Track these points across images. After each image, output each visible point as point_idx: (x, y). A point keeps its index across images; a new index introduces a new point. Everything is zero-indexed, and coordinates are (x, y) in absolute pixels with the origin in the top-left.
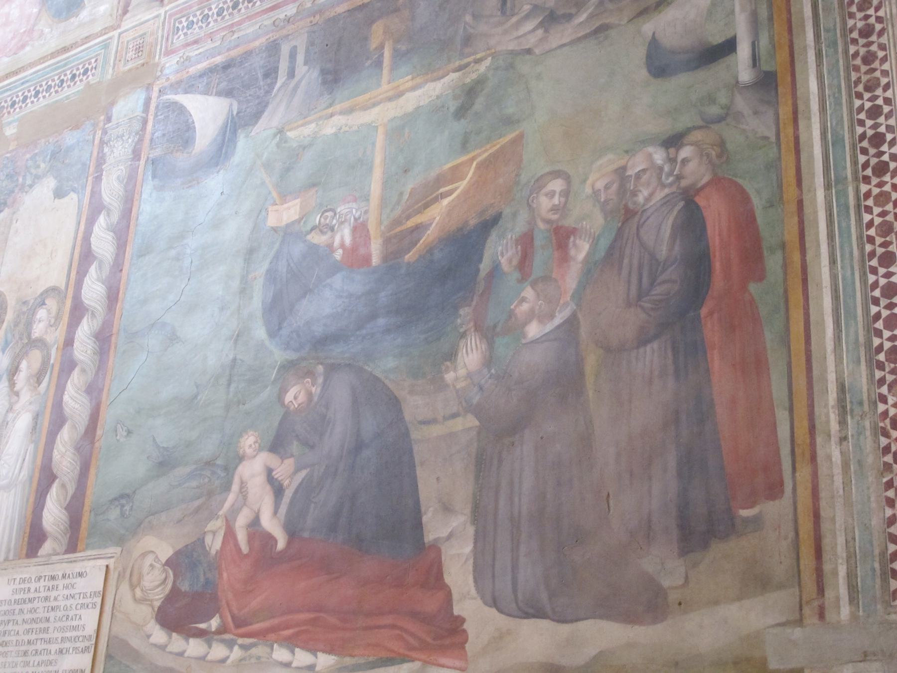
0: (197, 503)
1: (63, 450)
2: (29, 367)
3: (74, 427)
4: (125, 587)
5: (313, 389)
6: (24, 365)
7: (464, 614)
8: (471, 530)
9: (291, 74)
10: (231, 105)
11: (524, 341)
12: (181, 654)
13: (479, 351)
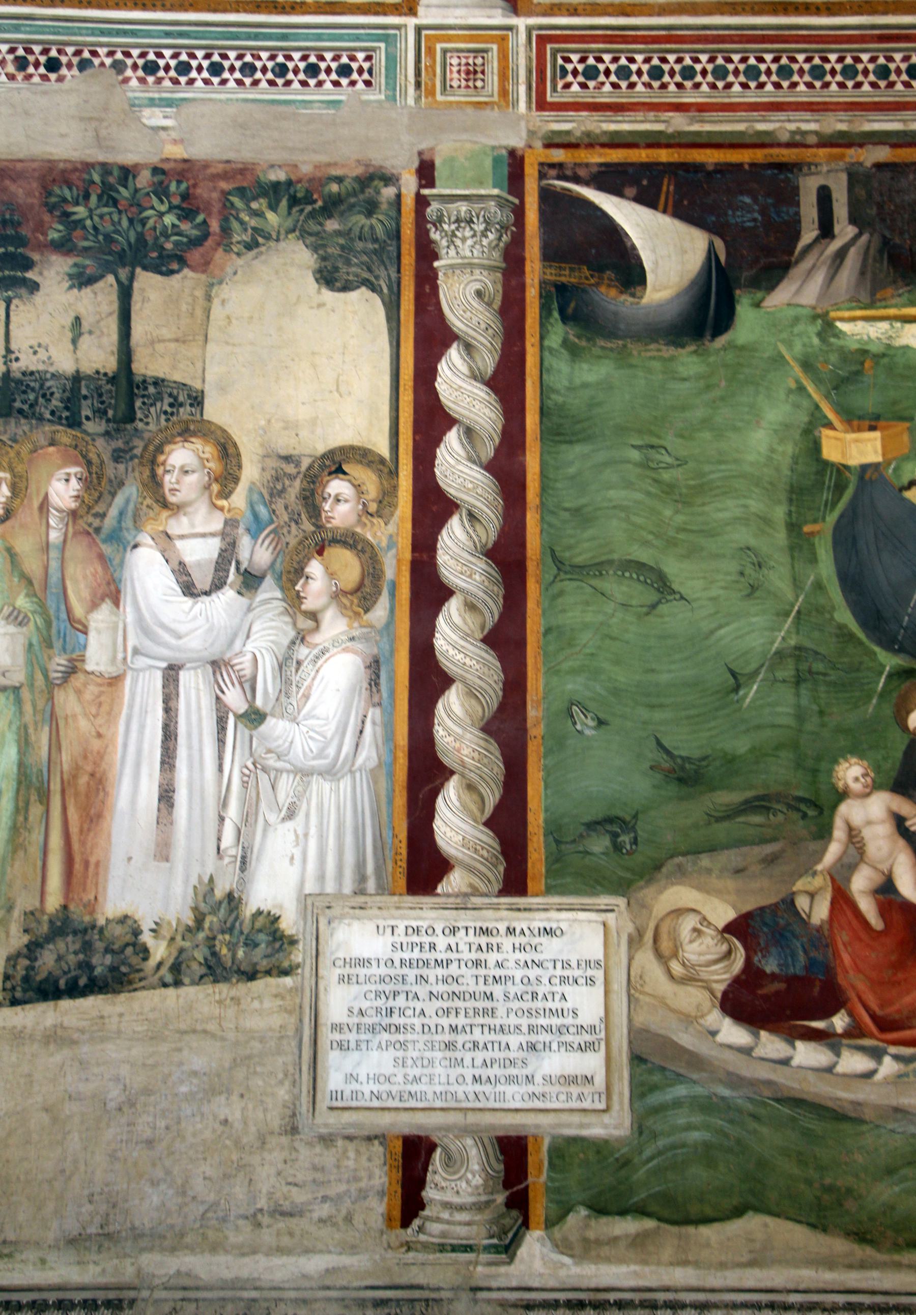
0: (769, 849)
1: (459, 730)
2: (331, 574)
3: (471, 693)
4: (646, 958)
6: (315, 568)
9: (826, 230)
10: (711, 245)
12: (785, 1062)
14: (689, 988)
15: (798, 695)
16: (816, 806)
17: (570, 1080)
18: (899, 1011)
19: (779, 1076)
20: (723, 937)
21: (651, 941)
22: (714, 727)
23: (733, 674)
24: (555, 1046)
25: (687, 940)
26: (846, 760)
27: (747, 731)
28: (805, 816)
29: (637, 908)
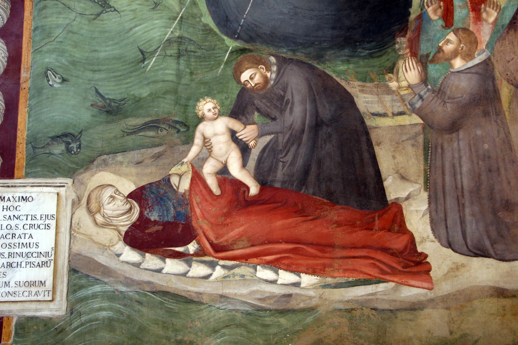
4: (82, 213)
5: (269, 75)
7: (426, 252)
8: (425, 195)
11: (452, 70)
12: (159, 271)
13: (416, 71)
14: (106, 230)
15: (178, 63)
16: (185, 125)
17: (31, 284)
18: (226, 241)
19: (156, 279)
20: (127, 201)
21: (85, 203)
22: (129, 82)
23: (142, 52)
24: (24, 264)
25: (106, 202)
26: (204, 100)
27: (149, 84)
28: (179, 131)
29: (78, 184)
